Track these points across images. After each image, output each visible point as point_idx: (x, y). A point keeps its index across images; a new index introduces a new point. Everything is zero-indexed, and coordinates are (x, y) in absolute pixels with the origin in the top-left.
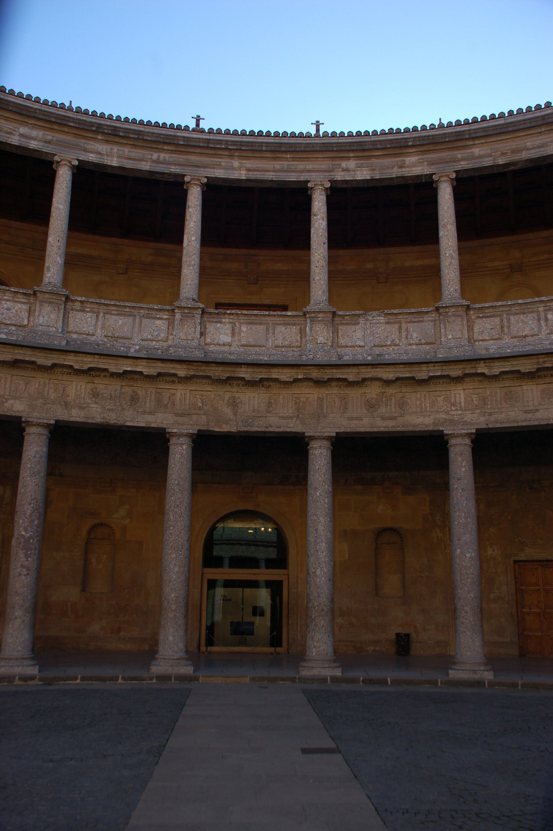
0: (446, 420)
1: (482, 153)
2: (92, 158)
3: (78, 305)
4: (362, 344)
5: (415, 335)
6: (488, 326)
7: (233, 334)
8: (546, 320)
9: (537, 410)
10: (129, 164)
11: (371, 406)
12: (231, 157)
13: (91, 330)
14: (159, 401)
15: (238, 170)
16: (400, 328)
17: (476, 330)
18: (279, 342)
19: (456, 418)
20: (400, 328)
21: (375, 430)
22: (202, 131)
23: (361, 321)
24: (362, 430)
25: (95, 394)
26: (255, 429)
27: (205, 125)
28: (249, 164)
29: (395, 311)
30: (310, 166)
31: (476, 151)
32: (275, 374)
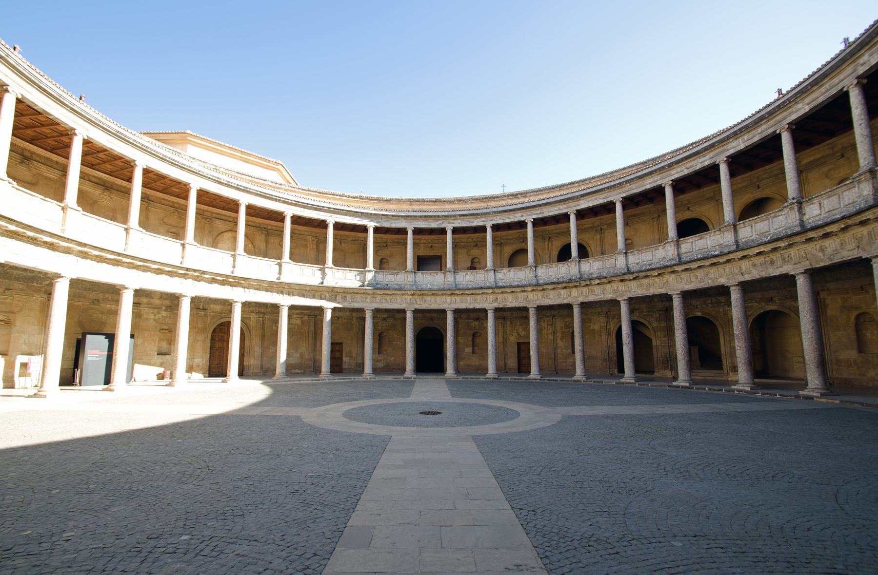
2: (732, 151)
3: (742, 225)
7: (820, 208)
10: (749, 143)
12: (797, 103)
13: (750, 234)
14: (784, 260)
15: (802, 108)
18: (846, 203)
22: (784, 95)
25: (754, 265)
26: (836, 261)
27: (851, 40)
28: (807, 100)
30: (841, 76)
32: (828, 229)
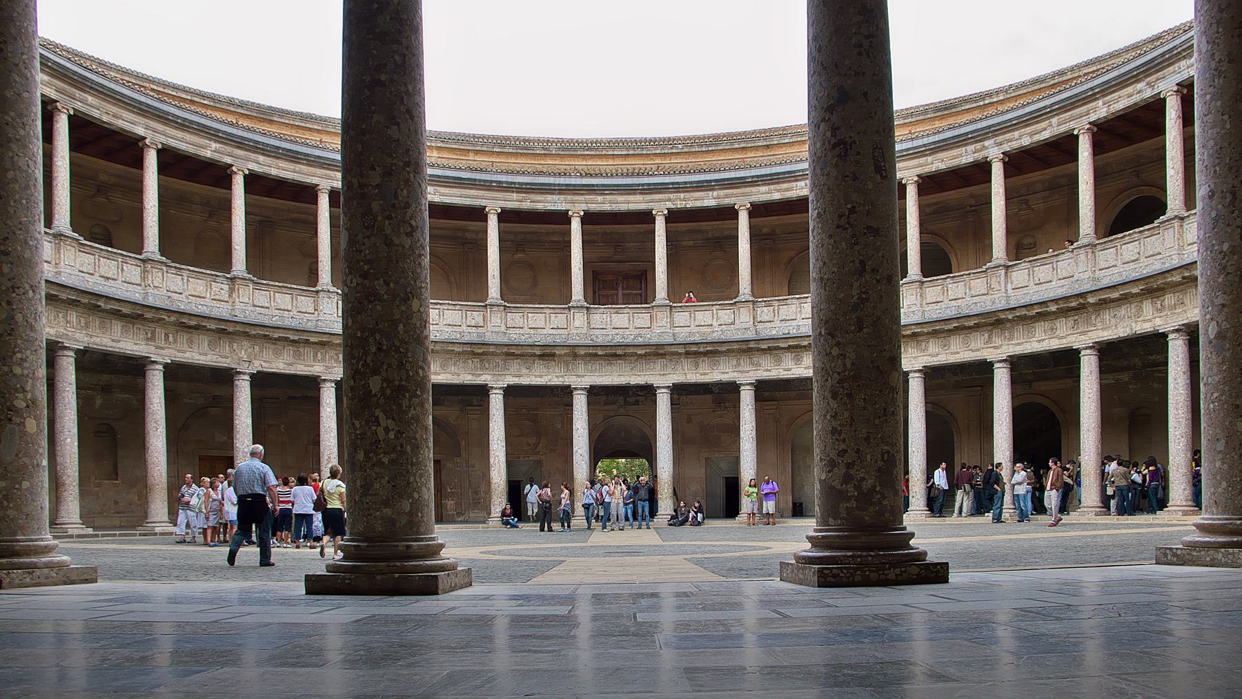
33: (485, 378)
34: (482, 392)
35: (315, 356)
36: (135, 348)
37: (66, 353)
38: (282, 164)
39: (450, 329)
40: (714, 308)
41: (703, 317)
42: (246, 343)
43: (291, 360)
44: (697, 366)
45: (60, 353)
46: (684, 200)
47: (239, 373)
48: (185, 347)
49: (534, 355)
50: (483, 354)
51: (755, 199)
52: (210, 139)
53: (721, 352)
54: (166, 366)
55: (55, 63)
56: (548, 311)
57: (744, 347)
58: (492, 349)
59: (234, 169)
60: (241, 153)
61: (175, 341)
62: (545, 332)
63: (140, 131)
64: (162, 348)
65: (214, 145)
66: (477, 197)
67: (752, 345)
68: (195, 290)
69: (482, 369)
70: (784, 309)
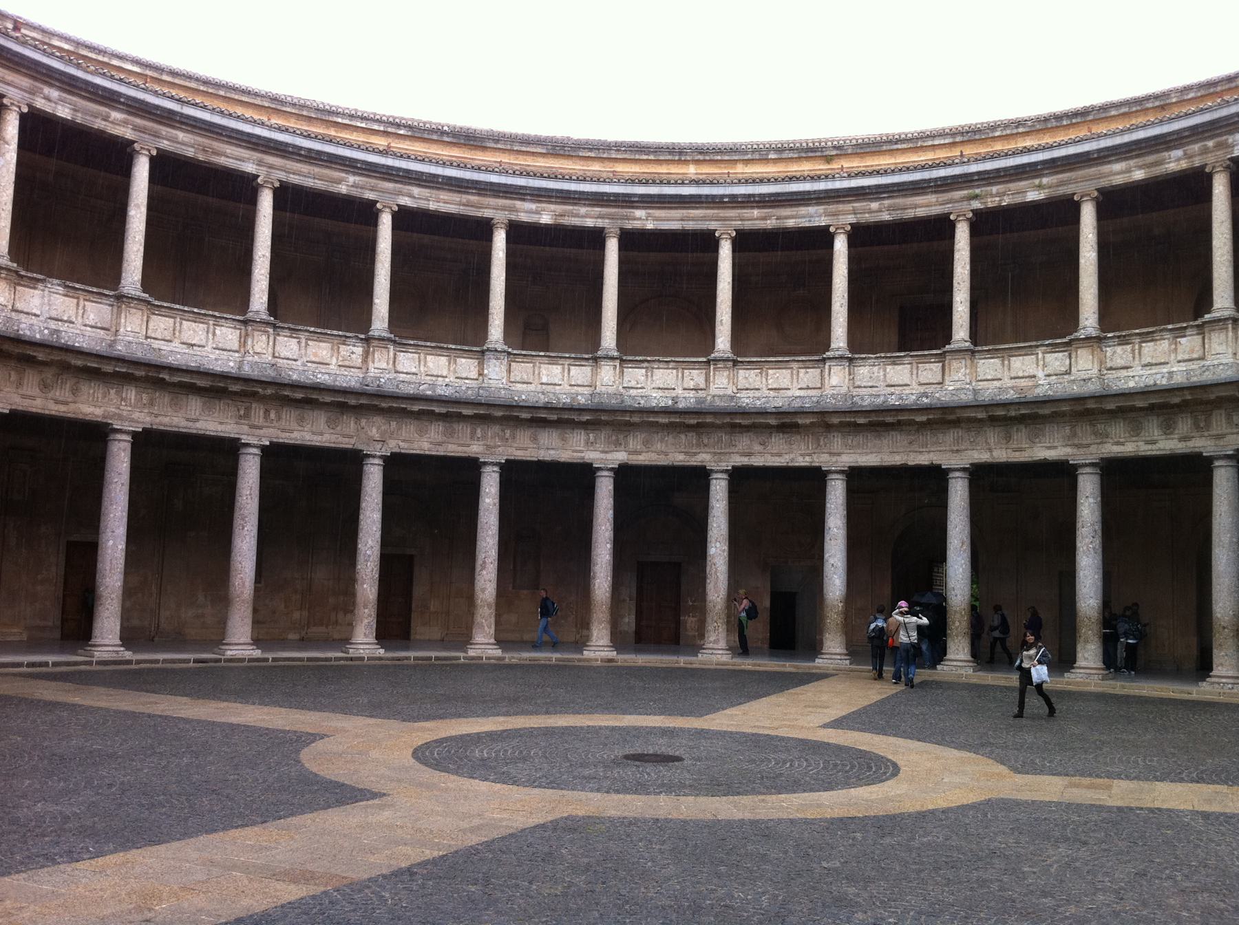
0: (115, 414)
1: (186, 139)
4: (38, 312)
5: (92, 316)
6: (162, 326)
8: (214, 334)
9: (198, 420)
11: (45, 386)
16: (78, 304)
17: (151, 325)
19: (125, 413)
20: (78, 304)
21: (47, 412)
23: (40, 286)
24: (34, 410)
29: (77, 286)
31: (181, 135)
33: (703, 458)
34: (701, 476)
35: (473, 434)
36: (220, 428)
37: (119, 436)
38: (444, 195)
39: (660, 393)
40: (1040, 351)
41: (1023, 365)
42: (378, 420)
43: (440, 438)
44: (1008, 438)
45: (111, 437)
46: (998, 195)
47: (368, 456)
48: (294, 425)
49: (768, 426)
50: (699, 425)
51: (1104, 183)
52: (347, 172)
53: (1044, 417)
54: (264, 449)
55: (129, 98)
56: (795, 365)
57: (1079, 408)
58: (709, 420)
59: (379, 206)
60: (390, 185)
61: (279, 418)
62: (789, 393)
63: (250, 168)
64: (260, 428)
65: (352, 179)
66: (704, 219)
67: (1091, 405)
68: (315, 355)
69: (698, 445)
70: (1148, 348)
